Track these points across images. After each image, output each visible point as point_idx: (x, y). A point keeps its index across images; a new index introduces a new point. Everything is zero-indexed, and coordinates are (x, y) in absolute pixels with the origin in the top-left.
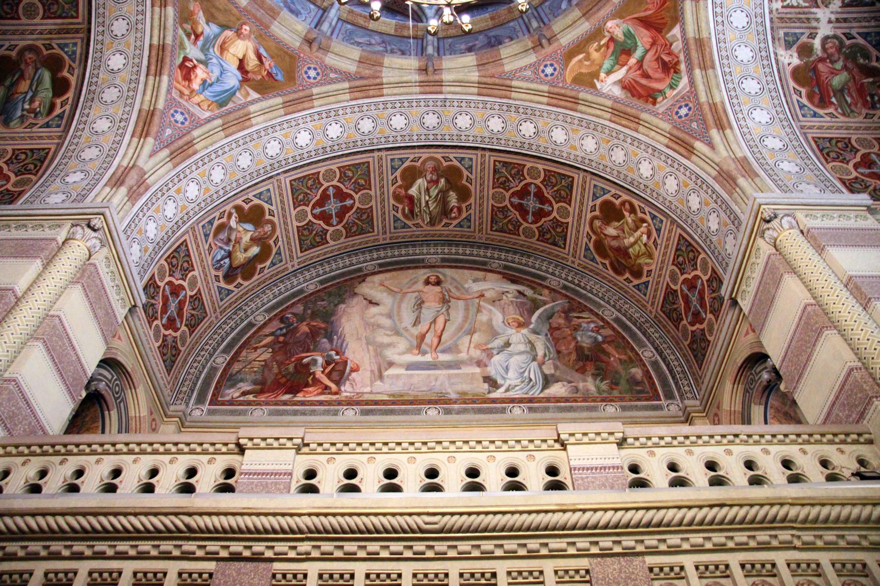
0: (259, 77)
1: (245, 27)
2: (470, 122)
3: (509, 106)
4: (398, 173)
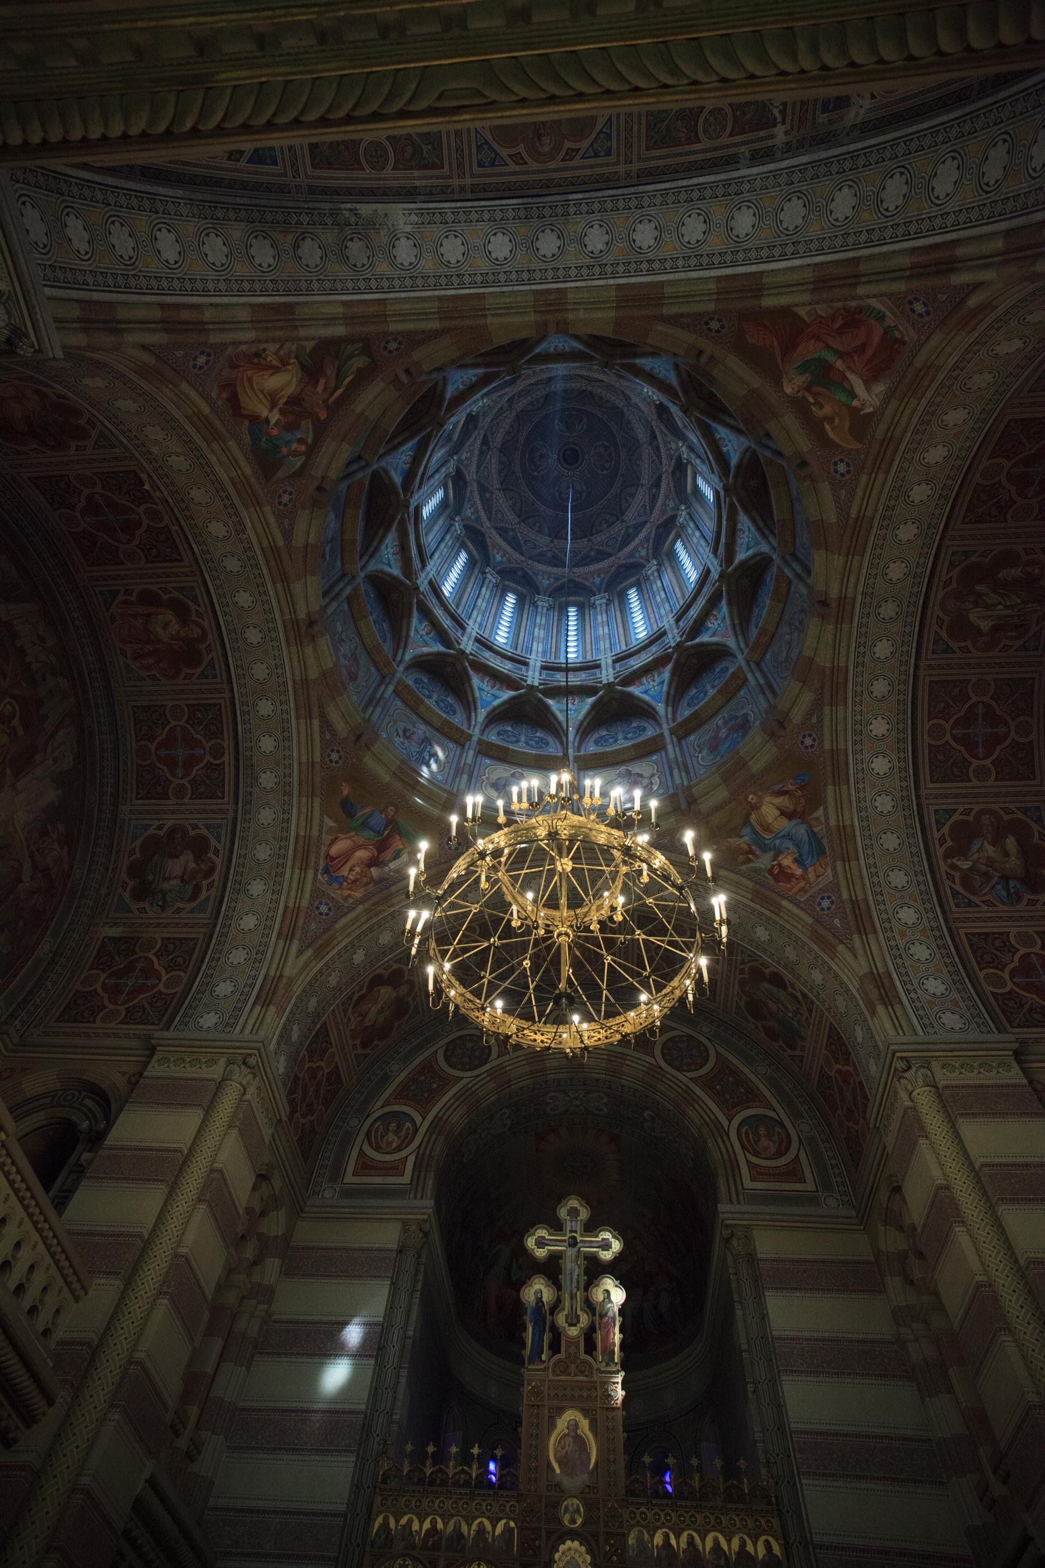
0: (802, 800)
1: (749, 799)
2: (898, 563)
3: (884, 518)
4: (955, 645)
